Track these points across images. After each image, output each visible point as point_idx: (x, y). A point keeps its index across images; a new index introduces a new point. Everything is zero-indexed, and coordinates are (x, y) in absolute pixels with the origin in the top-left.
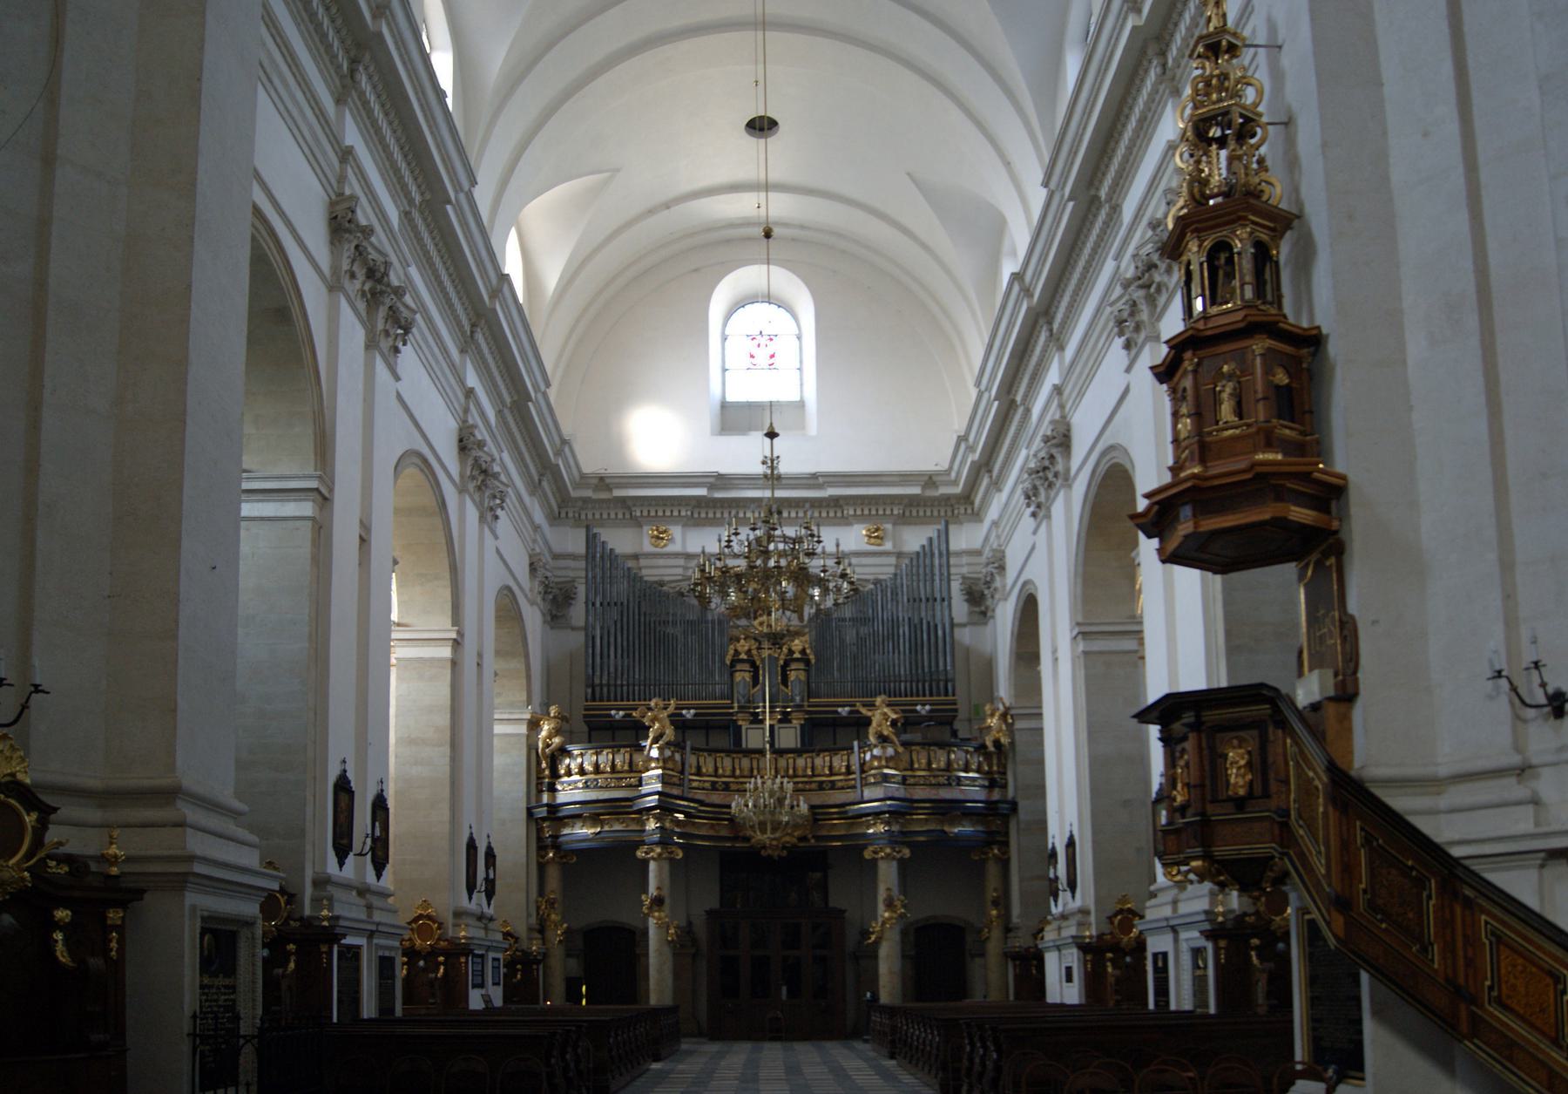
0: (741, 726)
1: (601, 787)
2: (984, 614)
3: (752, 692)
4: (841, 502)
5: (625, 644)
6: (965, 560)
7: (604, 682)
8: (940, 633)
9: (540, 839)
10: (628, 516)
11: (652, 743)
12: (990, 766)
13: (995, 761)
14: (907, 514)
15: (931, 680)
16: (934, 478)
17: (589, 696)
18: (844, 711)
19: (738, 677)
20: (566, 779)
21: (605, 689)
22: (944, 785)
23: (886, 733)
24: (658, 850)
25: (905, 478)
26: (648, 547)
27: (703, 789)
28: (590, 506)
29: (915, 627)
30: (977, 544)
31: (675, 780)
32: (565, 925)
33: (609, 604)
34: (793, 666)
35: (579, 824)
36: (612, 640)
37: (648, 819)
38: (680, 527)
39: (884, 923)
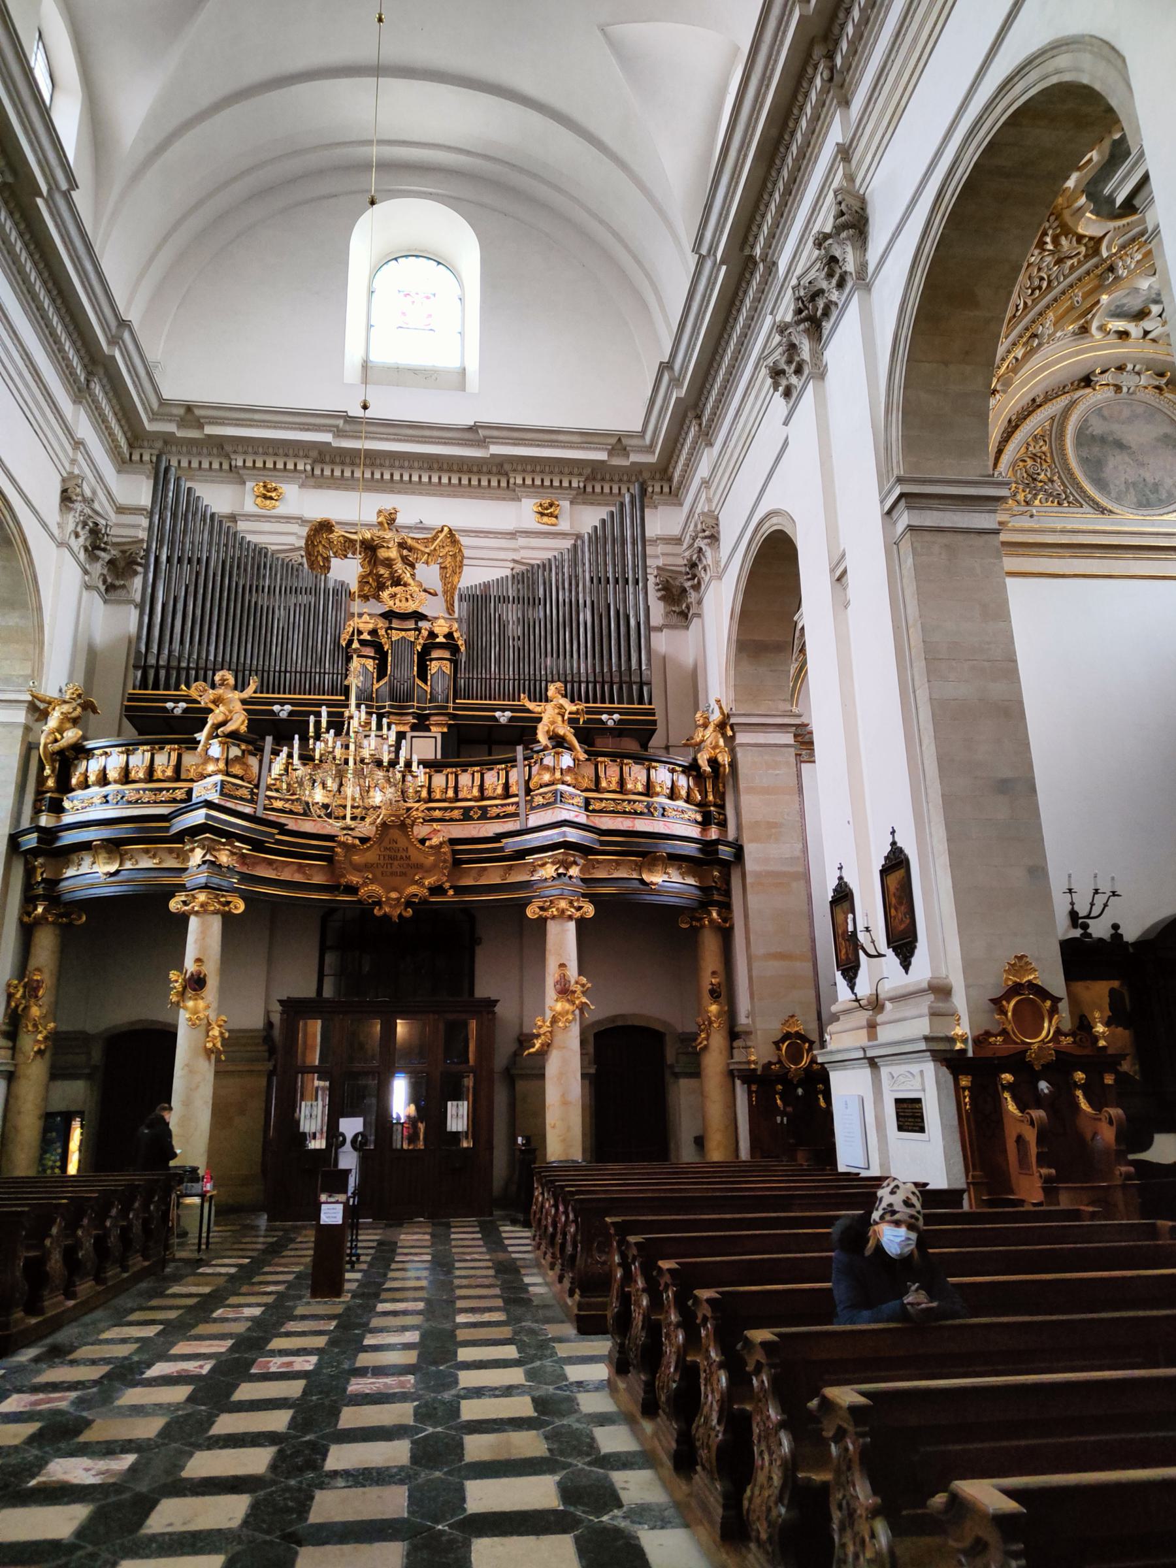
1: (130, 802)
2: (684, 615)
3: (376, 686)
4: (507, 467)
5: (199, 612)
6: (661, 548)
7: (161, 663)
8: (633, 622)
9: (28, 886)
10: (226, 466)
11: (211, 736)
12: (704, 793)
13: (710, 790)
14: (589, 489)
15: (621, 683)
16: (625, 441)
17: (138, 683)
18: (503, 717)
20: (79, 793)
21: (163, 673)
22: (642, 813)
23: (561, 732)
24: (202, 897)
25: (588, 438)
26: (250, 505)
27: (291, 812)
28: (174, 449)
29: (600, 614)
30: (676, 531)
31: (244, 793)
32: (52, 1025)
33: (180, 560)
34: (436, 654)
35: (87, 860)
36: (180, 606)
37: (192, 850)
39: (554, 1020)
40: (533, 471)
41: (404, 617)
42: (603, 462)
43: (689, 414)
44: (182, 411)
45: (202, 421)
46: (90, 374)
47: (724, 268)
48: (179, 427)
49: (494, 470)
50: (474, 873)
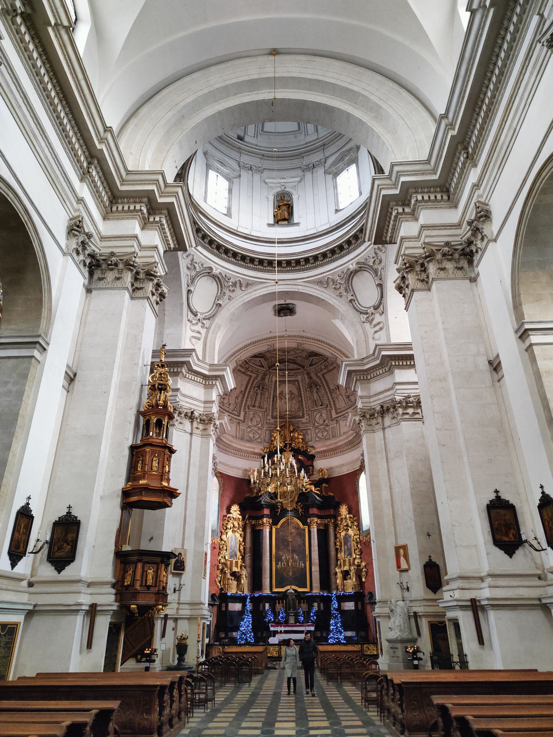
43: (460, 148)
46: (89, 163)
47: (492, 11)
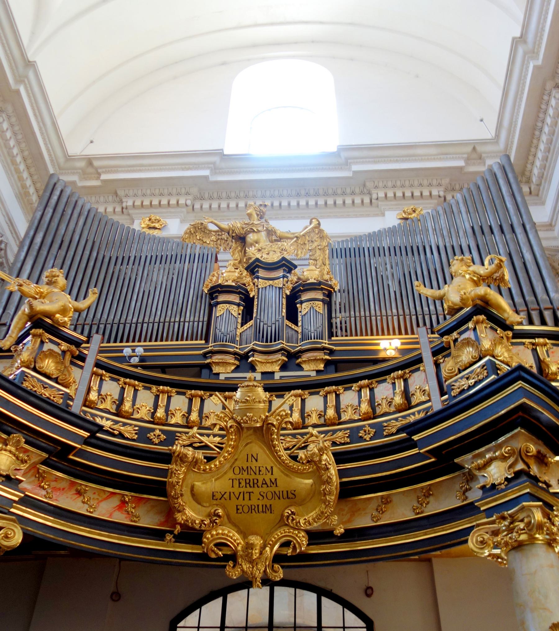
0: (218, 374)
4: (369, 185)
16: (479, 149)
19: (220, 310)
38: (178, 221)
40: (394, 187)
41: (271, 267)
42: (461, 168)
44: (82, 164)
45: (100, 171)
48: (81, 180)
49: (357, 190)
50: (372, 508)
